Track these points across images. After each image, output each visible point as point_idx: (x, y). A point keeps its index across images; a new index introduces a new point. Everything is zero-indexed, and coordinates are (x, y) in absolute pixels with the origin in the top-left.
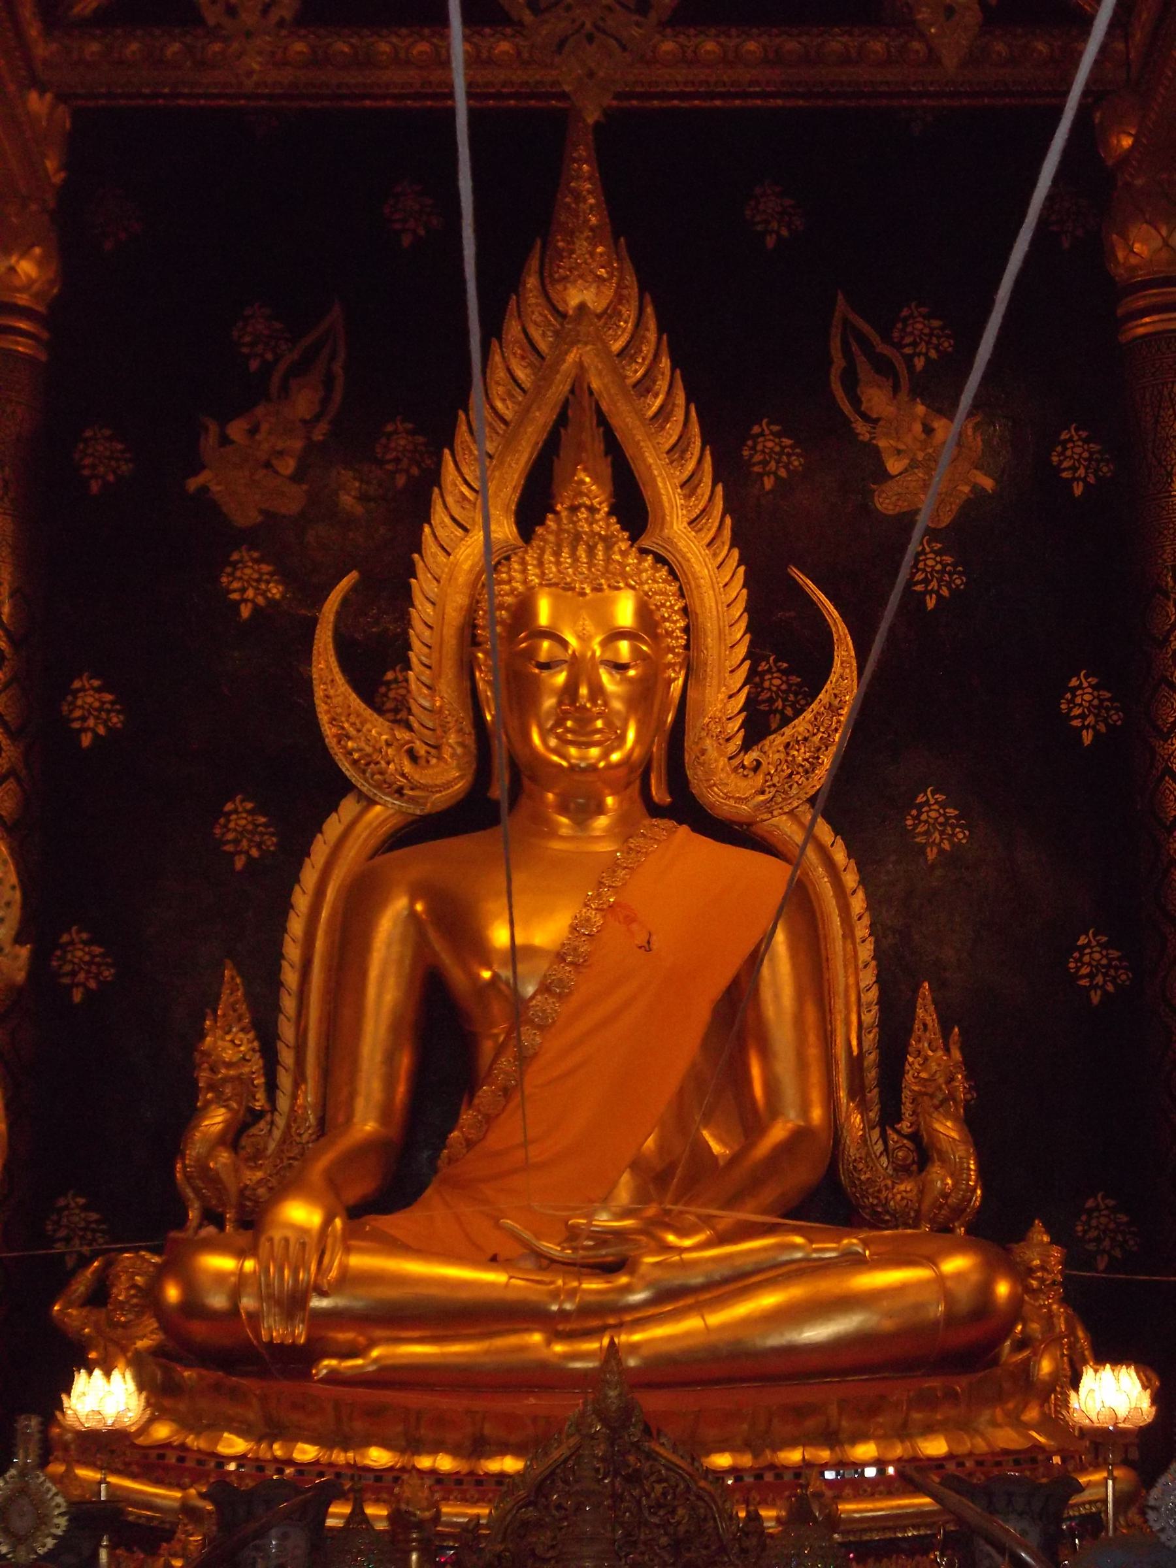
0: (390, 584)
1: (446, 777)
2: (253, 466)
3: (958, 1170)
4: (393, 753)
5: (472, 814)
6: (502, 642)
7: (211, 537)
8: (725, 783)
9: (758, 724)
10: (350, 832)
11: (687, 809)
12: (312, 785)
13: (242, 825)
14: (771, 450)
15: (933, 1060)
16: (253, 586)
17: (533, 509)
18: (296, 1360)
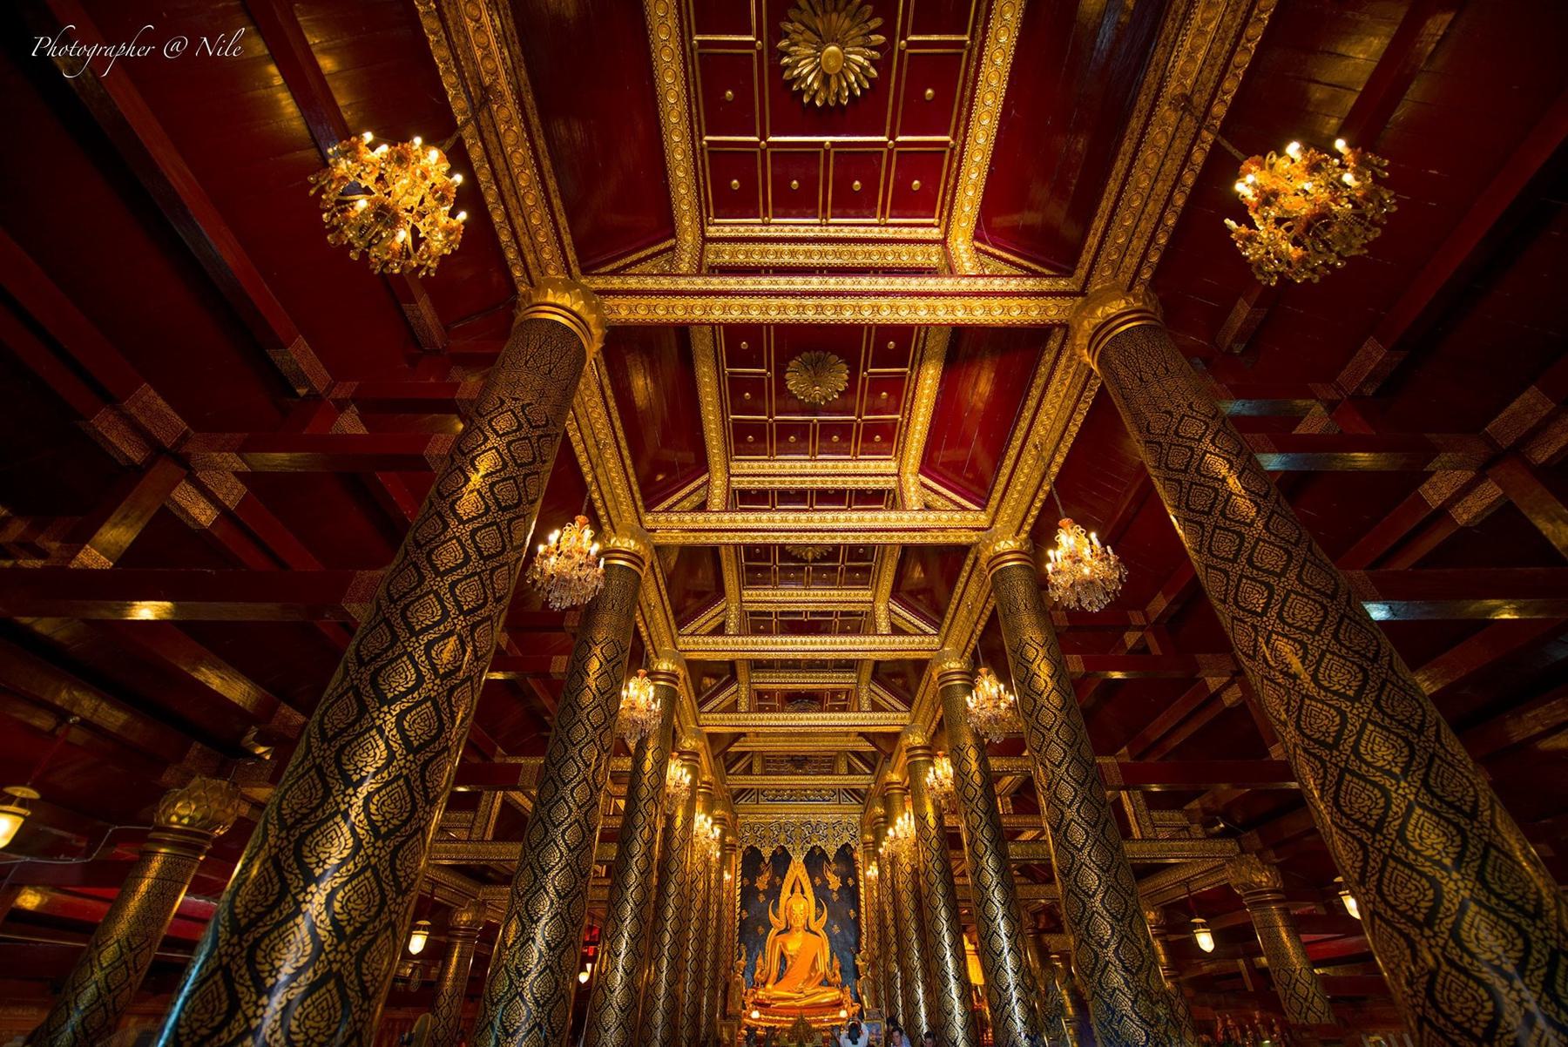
0: (777, 902)
1: (783, 926)
2: (762, 883)
3: (839, 978)
4: (778, 923)
5: (787, 930)
6: (789, 909)
7: (757, 891)
8: (813, 927)
9: (817, 917)
10: (773, 932)
11: (809, 930)
12: (769, 926)
13: (761, 930)
14: (818, 881)
15: (836, 963)
16: (762, 898)
17: (792, 891)
18: (768, 1006)
